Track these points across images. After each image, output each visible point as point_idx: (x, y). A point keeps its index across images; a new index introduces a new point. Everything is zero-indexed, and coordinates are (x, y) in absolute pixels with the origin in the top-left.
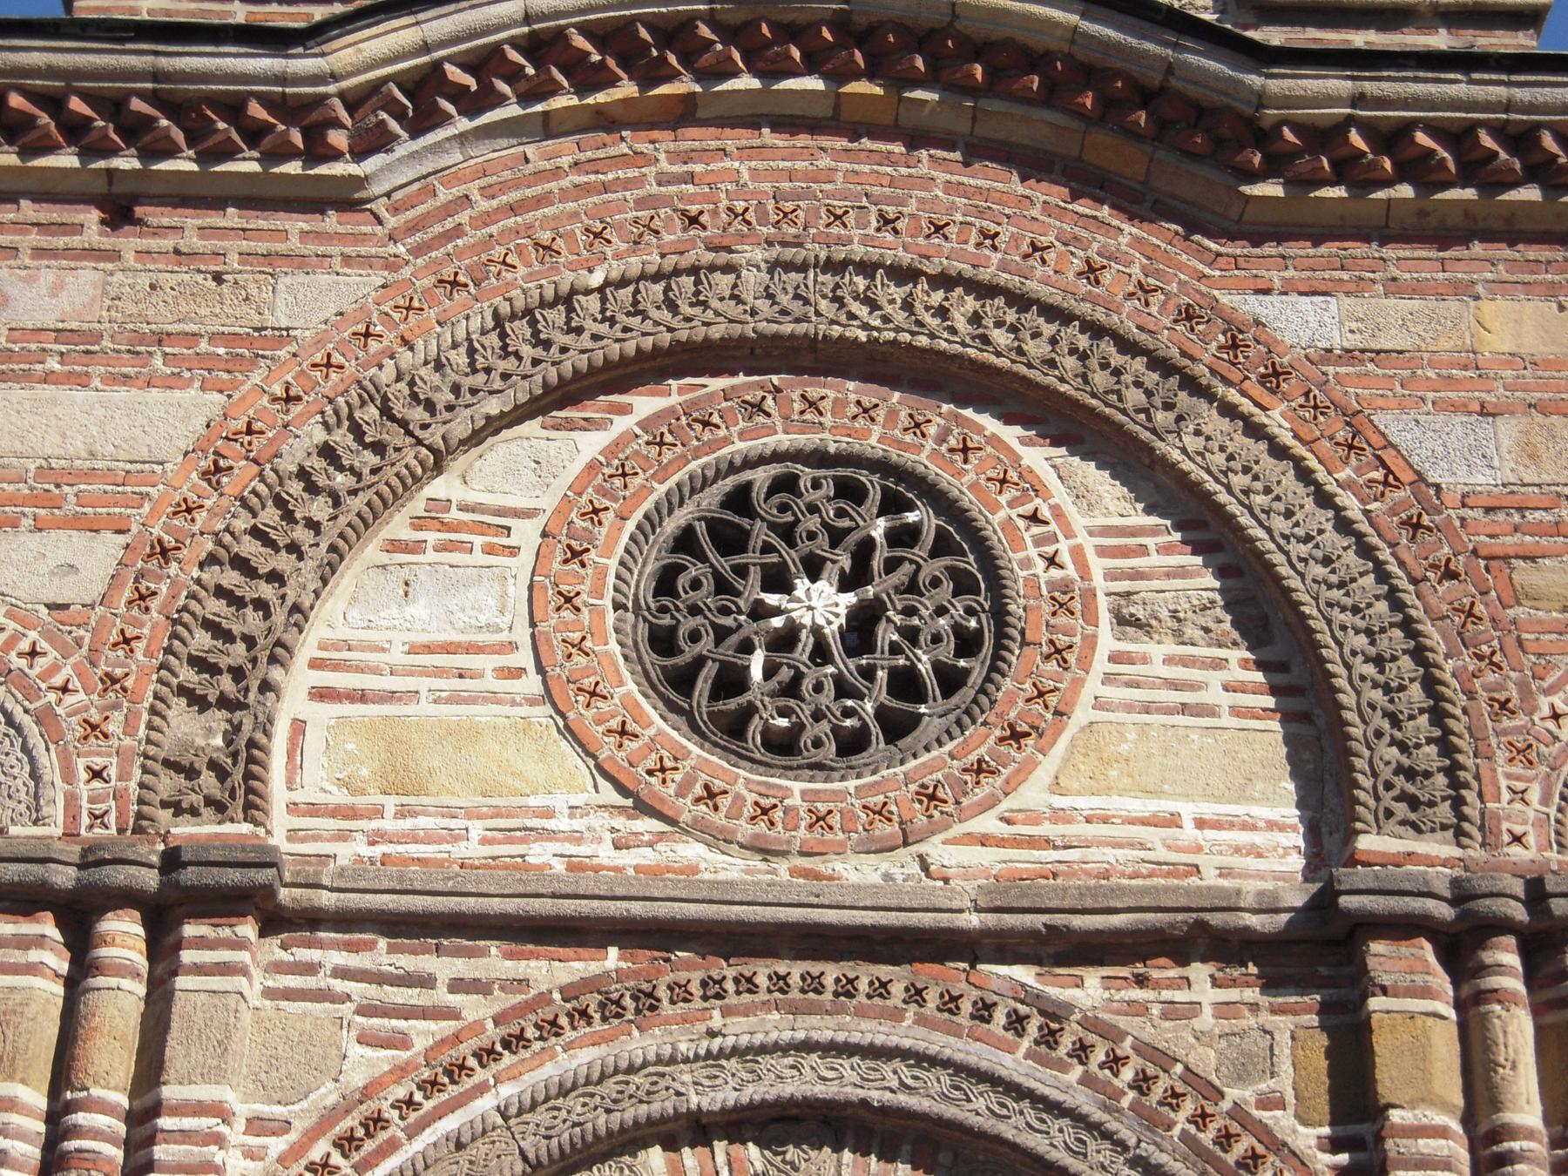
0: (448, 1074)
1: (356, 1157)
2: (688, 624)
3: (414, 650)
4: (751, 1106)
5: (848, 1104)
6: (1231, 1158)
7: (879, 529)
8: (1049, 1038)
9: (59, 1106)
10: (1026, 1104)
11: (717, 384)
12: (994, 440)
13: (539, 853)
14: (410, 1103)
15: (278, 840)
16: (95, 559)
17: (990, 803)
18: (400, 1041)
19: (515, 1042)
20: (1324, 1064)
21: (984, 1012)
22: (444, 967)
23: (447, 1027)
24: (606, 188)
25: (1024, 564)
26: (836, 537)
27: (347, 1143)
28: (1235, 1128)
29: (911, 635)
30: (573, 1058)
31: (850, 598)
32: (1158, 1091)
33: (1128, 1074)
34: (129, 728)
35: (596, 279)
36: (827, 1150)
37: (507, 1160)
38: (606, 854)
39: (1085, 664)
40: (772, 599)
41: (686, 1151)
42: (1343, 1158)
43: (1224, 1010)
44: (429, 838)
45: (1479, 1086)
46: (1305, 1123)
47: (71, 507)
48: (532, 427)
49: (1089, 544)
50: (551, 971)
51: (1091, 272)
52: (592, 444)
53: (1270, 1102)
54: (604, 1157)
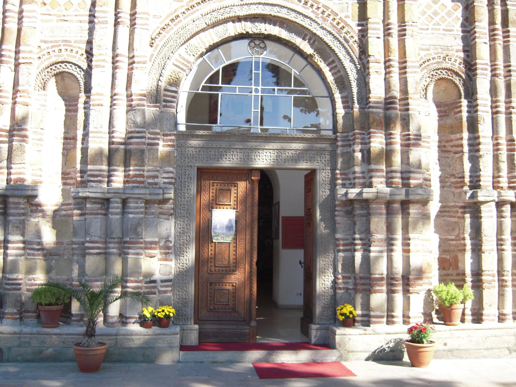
1: (174, 23)
4: (249, 15)
5: (267, 15)
6: (339, 27)
9: (117, 13)
10: (301, 16)
20: (358, 10)
28: (340, 22)
32: (326, 14)
33: (320, 11)
36: (263, 24)
37: (203, 24)
41: (236, 23)
42: (360, 28)
45: (386, 15)
46: (353, 21)
53: (346, 17)
54: (221, 24)
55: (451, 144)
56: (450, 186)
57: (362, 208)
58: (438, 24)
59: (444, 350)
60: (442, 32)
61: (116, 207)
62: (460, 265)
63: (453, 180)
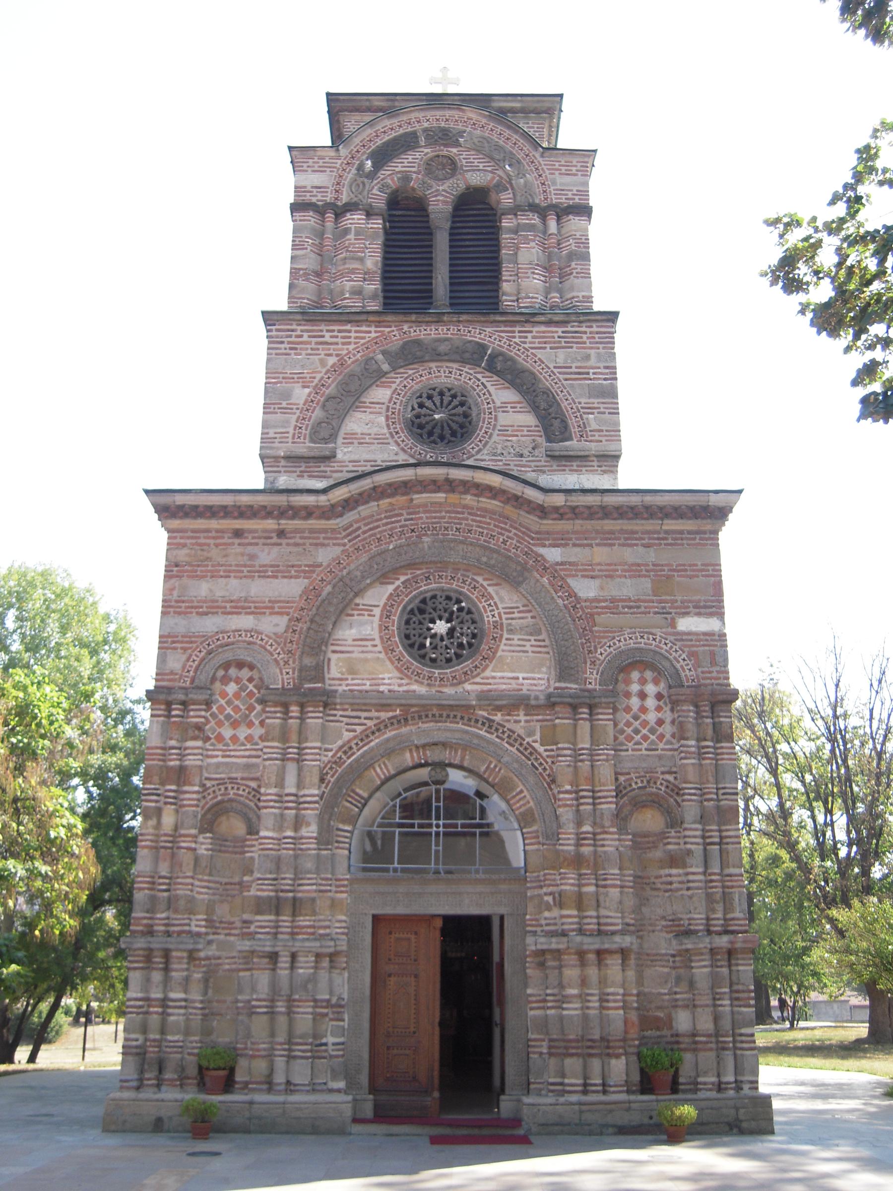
0: (365, 737)
2: (413, 632)
3: (354, 640)
7: (455, 608)
8: (490, 727)
11: (418, 572)
12: (482, 585)
13: (382, 688)
14: (357, 744)
15: (327, 687)
16: (283, 621)
17: (479, 674)
18: (354, 731)
19: (379, 730)
21: (477, 721)
22: (364, 714)
23: (363, 727)
24: (393, 523)
25: (488, 618)
26: (445, 611)
27: (345, 753)
29: (462, 634)
30: (389, 734)
31: (449, 625)
34: (294, 662)
35: (391, 547)
38: (396, 688)
39: (500, 641)
40: (431, 625)
43: (526, 721)
44: (358, 685)
47: (276, 610)
48: (377, 584)
49: (502, 611)
50: (384, 715)
51: (504, 542)
52: (390, 588)
55: (660, 880)
56: (661, 931)
57: (554, 959)
58: (640, 744)
59: (650, 1125)
60: (644, 752)
61: (284, 961)
62: (674, 1024)
63: (664, 923)
